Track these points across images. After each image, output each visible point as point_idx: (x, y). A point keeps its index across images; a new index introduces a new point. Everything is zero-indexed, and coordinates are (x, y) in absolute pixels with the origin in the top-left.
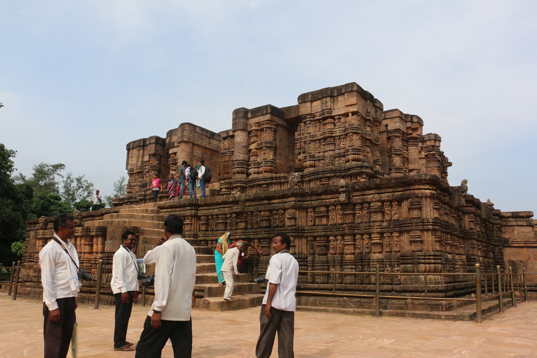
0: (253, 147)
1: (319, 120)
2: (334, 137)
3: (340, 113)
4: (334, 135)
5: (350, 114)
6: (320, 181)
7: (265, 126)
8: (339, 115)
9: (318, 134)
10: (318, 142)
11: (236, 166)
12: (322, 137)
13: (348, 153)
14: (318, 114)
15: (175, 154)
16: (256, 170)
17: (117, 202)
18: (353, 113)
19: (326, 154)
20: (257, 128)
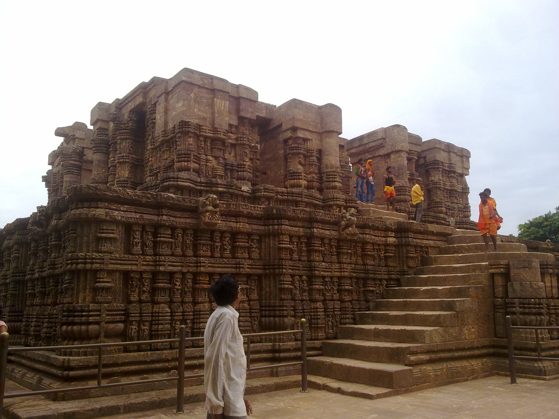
15: (305, 140)
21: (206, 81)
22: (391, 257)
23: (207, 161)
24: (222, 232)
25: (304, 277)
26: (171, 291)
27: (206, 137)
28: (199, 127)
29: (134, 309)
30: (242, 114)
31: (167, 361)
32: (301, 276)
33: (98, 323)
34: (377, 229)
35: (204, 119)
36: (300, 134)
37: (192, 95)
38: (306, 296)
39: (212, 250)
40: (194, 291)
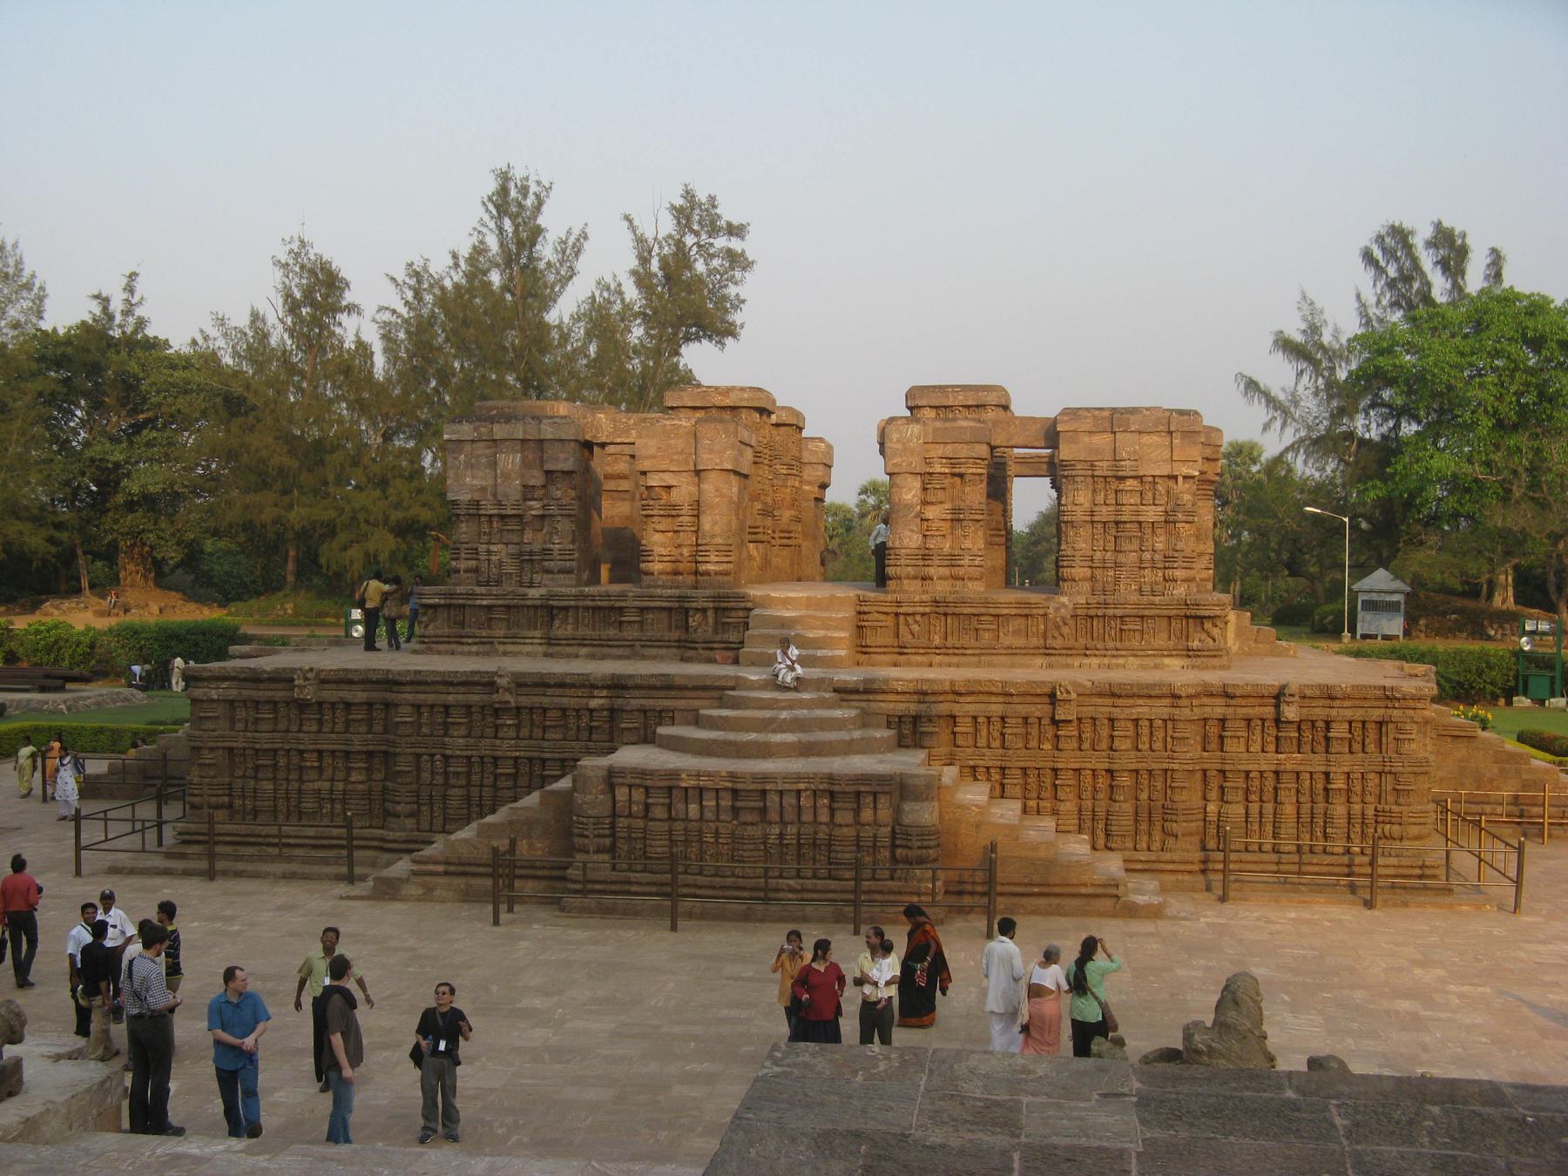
0: (931, 512)
1: (1105, 477)
2: (1140, 523)
3: (1157, 473)
4: (1141, 519)
5: (1180, 479)
6: (1123, 622)
7: (971, 471)
8: (1154, 476)
9: (1104, 509)
10: (1099, 526)
11: (903, 562)
12: (1112, 518)
13: (1176, 565)
14: (1105, 464)
16: (945, 571)
17: (442, 602)
18: (1185, 478)
19: (1121, 558)
20: (947, 471)
21: (483, 430)
22: (597, 728)
23: (489, 552)
24: (333, 704)
25: (438, 757)
26: (275, 767)
27: (490, 516)
28: (476, 504)
29: (238, 783)
30: (548, 467)
31: (260, 836)
32: (432, 756)
33: (201, 796)
34: (573, 686)
35: (483, 489)
36: (654, 480)
37: (462, 457)
38: (439, 780)
39: (320, 722)
40: (301, 769)
